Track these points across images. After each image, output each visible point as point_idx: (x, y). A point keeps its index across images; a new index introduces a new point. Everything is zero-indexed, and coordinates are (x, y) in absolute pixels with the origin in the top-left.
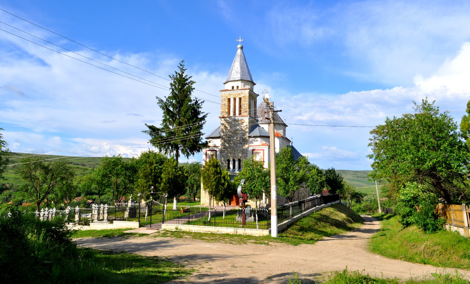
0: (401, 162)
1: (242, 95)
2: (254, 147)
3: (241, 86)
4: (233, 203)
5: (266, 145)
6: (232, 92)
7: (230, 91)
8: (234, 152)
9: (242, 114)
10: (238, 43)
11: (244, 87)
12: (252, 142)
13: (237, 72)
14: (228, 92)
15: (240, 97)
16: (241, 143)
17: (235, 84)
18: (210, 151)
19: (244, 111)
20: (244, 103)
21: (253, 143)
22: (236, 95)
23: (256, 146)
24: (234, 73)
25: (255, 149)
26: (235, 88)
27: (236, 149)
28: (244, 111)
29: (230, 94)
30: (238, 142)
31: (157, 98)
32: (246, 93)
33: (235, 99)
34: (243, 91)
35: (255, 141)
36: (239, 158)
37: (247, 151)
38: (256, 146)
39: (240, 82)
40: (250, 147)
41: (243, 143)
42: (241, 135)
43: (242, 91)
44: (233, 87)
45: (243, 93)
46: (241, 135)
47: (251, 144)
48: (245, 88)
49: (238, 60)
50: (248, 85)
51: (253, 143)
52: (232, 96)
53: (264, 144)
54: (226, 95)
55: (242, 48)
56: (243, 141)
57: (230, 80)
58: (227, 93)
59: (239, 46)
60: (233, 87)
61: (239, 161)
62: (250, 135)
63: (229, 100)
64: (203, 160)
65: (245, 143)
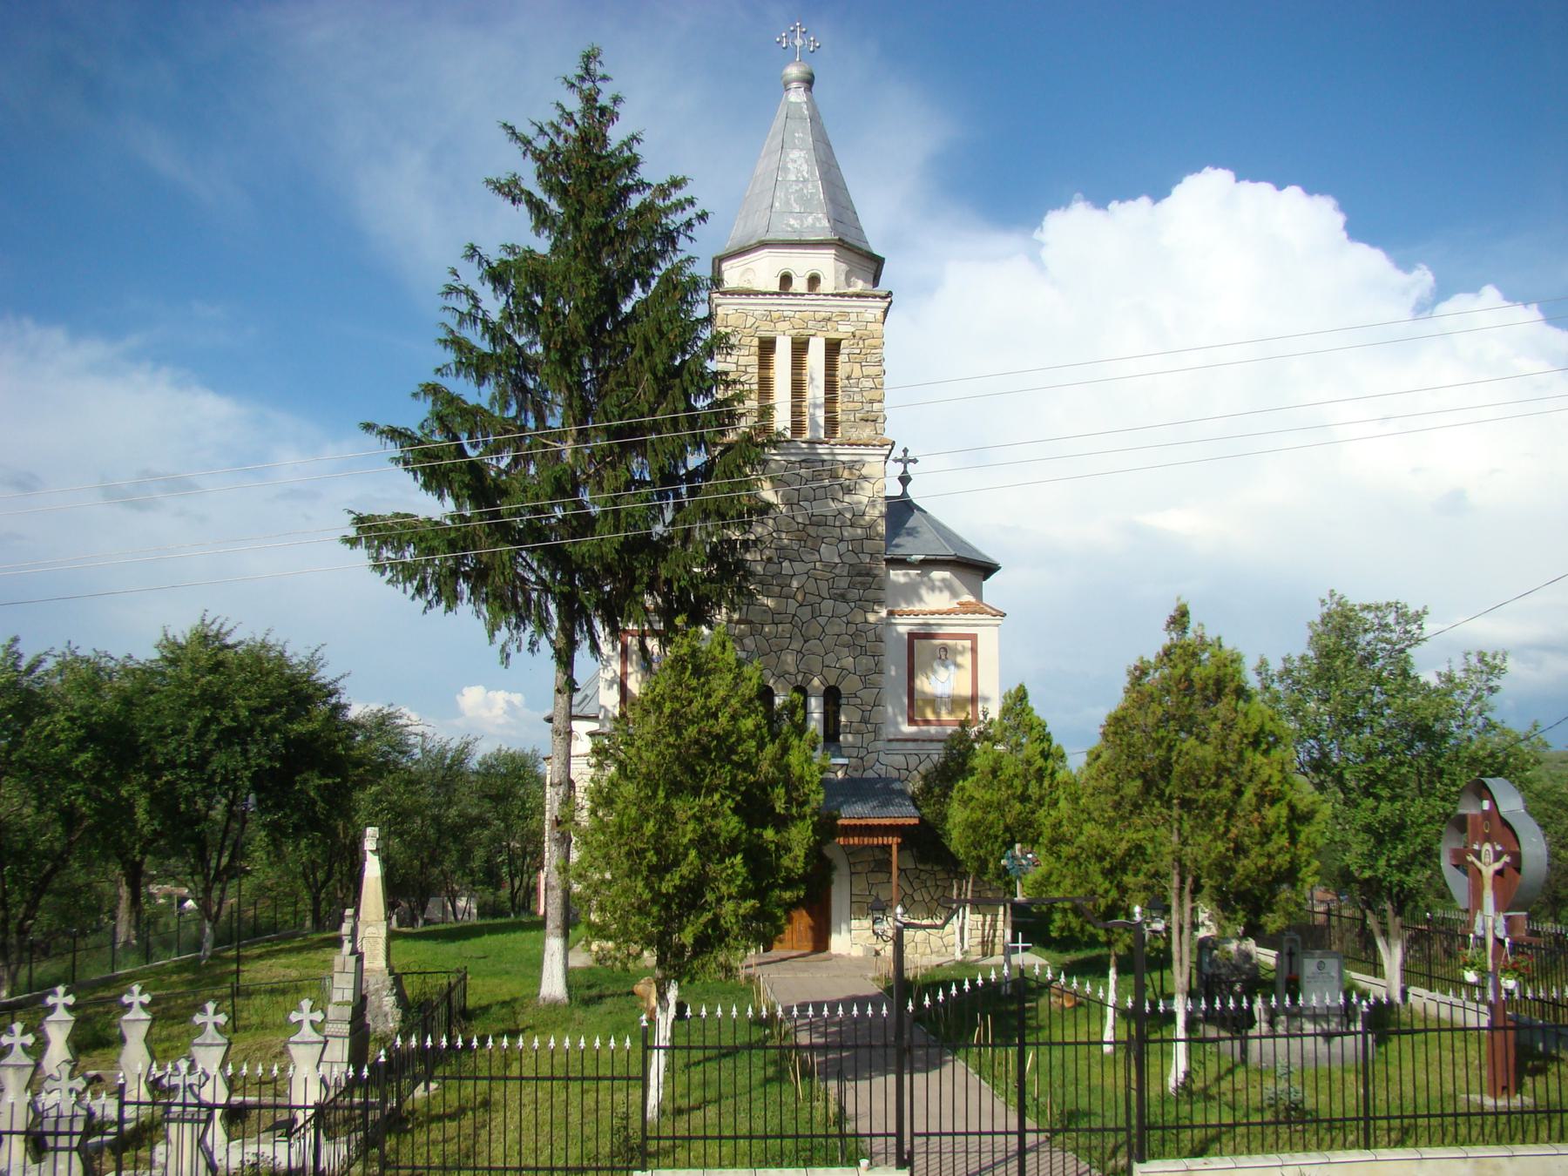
1: (841, 328)
3: (837, 278)
5: (988, 613)
6: (784, 305)
7: (768, 300)
8: (795, 646)
10: (789, 54)
11: (849, 286)
12: (911, 592)
13: (805, 201)
14: (760, 300)
15: (833, 335)
16: (843, 597)
17: (802, 264)
18: (497, 633)
20: (857, 372)
21: (920, 599)
22: (811, 324)
23: (933, 613)
24: (788, 202)
26: (799, 285)
27: (814, 629)
29: (775, 315)
30: (824, 585)
32: (870, 317)
33: (800, 348)
34: (855, 302)
35: (932, 588)
36: (832, 683)
37: (879, 639)
38: (933, 613)
39: (829, 254)
41: (854, 594)
42: (843, 547)
43: (846, 302)
44: (786, 280)
45: (853, 317)
47: (909, 602)
48: (851, 290)
49: (803, 140)
50: (865, 281)
51: (920, 599)
52: (781, 326)
53: (970, 603)
54: (750, 321)
55: (809, 82)
56: (851, 586)
57: (770, 237)
58: (757, 306)
59: (793, 71)
60: (786, 280)
61: (832, 697)
63: (767, 347)
65: (870, 594)
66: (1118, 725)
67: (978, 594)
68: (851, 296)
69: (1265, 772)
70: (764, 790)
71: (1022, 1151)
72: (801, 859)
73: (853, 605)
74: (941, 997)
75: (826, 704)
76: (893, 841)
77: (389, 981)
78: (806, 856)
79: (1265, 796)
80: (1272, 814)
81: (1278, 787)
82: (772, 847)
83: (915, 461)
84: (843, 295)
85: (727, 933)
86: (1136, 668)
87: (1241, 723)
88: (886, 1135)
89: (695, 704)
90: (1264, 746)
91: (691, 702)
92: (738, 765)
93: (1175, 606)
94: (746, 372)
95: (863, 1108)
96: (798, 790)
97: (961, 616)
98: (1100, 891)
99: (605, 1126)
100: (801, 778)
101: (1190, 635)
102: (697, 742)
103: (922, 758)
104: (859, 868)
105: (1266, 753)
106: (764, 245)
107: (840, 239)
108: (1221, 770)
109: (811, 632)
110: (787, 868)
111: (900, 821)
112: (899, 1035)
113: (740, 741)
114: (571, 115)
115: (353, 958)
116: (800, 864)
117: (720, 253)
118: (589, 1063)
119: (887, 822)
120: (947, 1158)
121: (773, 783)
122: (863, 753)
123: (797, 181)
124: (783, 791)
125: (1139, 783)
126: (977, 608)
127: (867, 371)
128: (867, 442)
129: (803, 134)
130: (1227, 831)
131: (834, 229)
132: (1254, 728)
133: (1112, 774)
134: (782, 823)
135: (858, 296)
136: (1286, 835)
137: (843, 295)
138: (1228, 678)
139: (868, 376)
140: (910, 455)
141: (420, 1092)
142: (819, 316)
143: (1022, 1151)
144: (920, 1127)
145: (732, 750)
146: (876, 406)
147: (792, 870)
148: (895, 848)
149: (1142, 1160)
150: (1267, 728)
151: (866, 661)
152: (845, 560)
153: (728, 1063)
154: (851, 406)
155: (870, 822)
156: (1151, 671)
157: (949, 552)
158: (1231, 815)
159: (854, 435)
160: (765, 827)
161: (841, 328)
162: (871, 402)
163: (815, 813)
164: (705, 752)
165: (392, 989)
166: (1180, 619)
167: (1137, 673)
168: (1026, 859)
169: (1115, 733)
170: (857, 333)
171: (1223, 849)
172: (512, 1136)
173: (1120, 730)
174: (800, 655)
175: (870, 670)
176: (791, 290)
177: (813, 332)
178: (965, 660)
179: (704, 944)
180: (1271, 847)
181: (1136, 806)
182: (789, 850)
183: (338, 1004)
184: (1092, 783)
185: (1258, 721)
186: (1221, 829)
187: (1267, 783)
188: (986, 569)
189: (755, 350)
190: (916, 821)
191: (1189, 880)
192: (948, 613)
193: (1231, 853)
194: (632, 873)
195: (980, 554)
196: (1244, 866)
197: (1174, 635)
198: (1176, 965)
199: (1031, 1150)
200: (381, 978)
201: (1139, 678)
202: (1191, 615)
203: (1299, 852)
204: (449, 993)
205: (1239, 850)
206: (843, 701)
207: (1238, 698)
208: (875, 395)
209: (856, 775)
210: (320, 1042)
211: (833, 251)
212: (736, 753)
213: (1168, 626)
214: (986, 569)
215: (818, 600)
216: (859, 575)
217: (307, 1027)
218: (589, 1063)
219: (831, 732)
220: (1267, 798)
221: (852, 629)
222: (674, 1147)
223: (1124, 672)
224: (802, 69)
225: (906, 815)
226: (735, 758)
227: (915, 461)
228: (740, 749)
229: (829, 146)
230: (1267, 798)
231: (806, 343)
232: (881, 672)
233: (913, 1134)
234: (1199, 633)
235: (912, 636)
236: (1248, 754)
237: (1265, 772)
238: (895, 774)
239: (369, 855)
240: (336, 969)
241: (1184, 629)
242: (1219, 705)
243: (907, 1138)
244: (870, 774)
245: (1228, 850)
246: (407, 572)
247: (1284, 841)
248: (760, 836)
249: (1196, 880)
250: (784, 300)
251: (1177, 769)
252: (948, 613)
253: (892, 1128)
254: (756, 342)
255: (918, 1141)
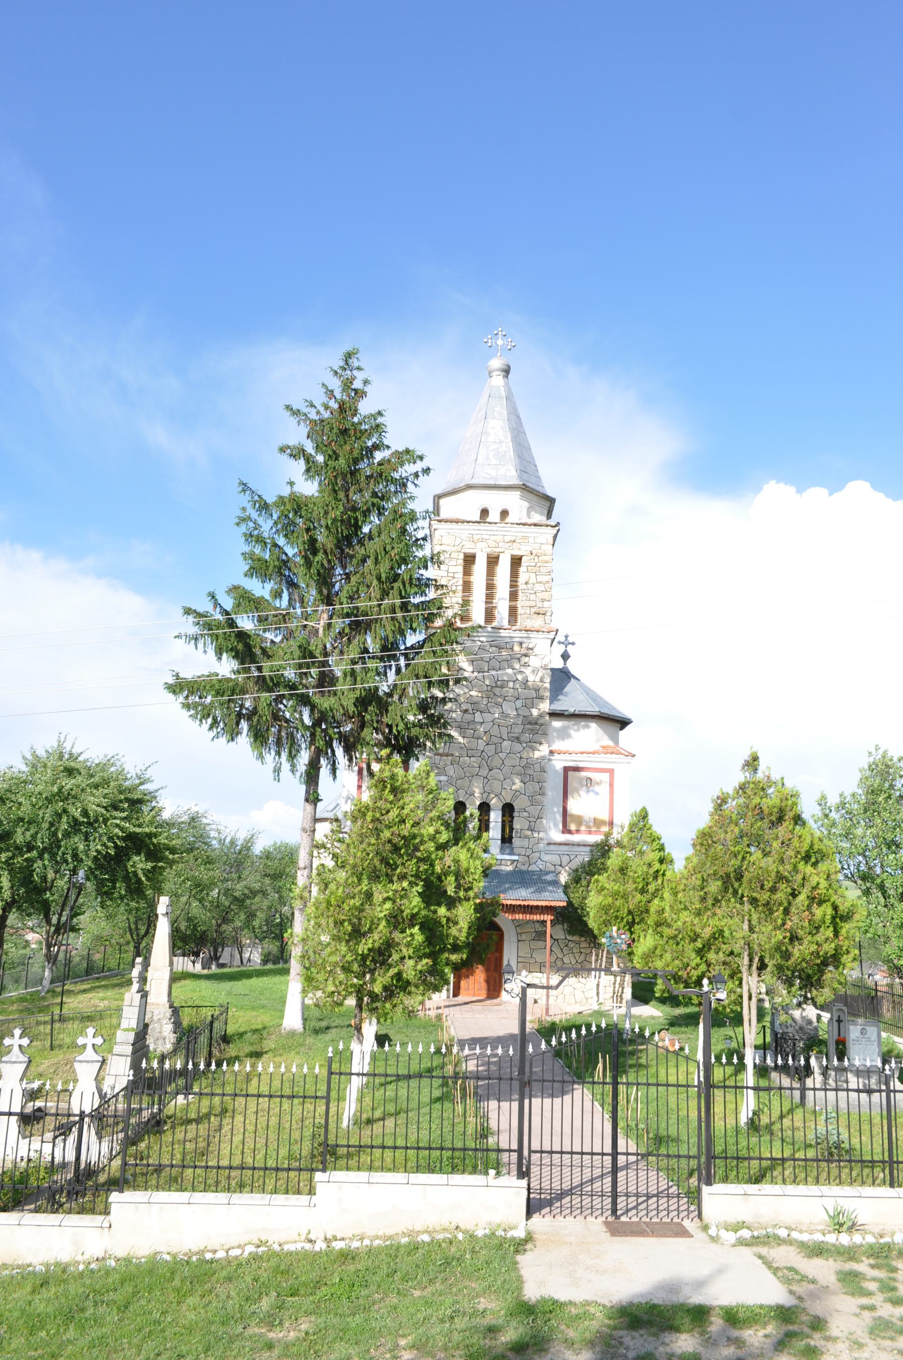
0: (884, 839)
1: (523, 548)
2: (574, 757)
4: (468, 989)
8: (484, 772)
9: (522, 621)
15: (517, 553)
17: (495, 501)
19: (533, 610)
20: (533, 580)
22: (501, 544)
23: (582, 753)
25: (581, 765)
26: (494, 516)
27: (496, 762)
28: (533, 610)
29: (476, 537)
30: (504, 731)
31: (244, 490)
33: (493, 561)
36: (508, 801)
38: (582, 753)
39: (517, 494)
40: (556, 756)
41: (526, 737)
42: (519, 703)
43: (526, 529)
44: (485, 512)
45: (531, 540)
46: (519, 703)
48: (530, 521)
50: (541, 514)
52: (480, 545)
53: (609, 747)
54: (458, 541)
55: (507, 371)
59: (496, 363)
60: (485, 512)
61: (508, 810)
62: (558, 707)
63: (469, 560)
64: (348, 798)
66: (705, 840)
67: (616, 740)
68: (530, 525)
69: (814, 880)
70: (439, 878)
71: (615, 1170)
72: (465, 930)
73: (524, 745)
74: (554, 1043)
75: (503, 816)
76: (548, 918)
77: (169, 1012)
78: (470, 928)
79: (815, 898)
80: (818, 912)
81: (824, 891)
82: (444, 921)
83: (573, 644)
84: (524, 524)
85: (408, 983)
86: (718, 798)
87: (795, 842)
88: (510, 1151)
89: (391, 813)
90: (813, 860)
91: (388, 812)
92: (420, 860)
93: (749, 753)
94: (454, 578)
95: (504, 1126)
96: (464, 879)
97: (603, 755)
98: (693, 964)
99: (308, 1133)
100: (467, 870)
101: (760, 775)
102: (390, 841)
103: (572, 857)
104: (524, 937)
105: (815, 865)
106: (469, 487)
107: (524, 484)
108: (780, 878)
109: (494, 764)
110: (455, 937)
111: (553, 904)
112: (522, 1071)
113: (422, 842)
114: (332, 391)
115: (139, 995)
116: (464, 934)
117: (439, 491)
118: (287, 1085)
119: (544, 904)
120: (556, 1170)
121: (446, 874)
122: (529, 852)
123: (495, 442)
124: (453, 878)
125: (719, 883)
126: (615, 750)
127: (540, 578)
128: (537, 628)
129: (501, 409)
130: (784, 924)
131: (520, 477)
132: (806, 847)
133: (699, 876)
134: (452, 903)
135: (535, 525)
136: (831, 929)
137: (524, 524)
138: (788, 808)
139: (540, 582)
140: (570, 640)
141: (181, 1099)
142: (507, 539)
143: (615, 1170)
144: (535, 1146)
145: (416, 849)
146: (546, 604)
147: (458, 939)
148: (549, 923)
149: (709, 1183)
150: (816, 847)
151: (532, 787)
152: (520, 712)
153: (414, 1083)
154: (528, 604)
155: (531, 903)
156: (730, 801)
157: (593, 709)
158: (786, 911)
159: (529, 624)
160: (439, 905)
161: (523, 548)
162: (543, 600)
163: (476, 897)
164: (396, 849)
165: (170, 1019)
166: (752, 763)
167: (719, 801)
168: (620, 939)
169: (702, 844)
170: (534, 552)
171: (781, 937)
172: (238, 1139)
173: (705, 842)
174: (486, 780)
175: (536, 792)
176: (488, 520)
177: (502, 550)
178: (604, 789)
179: (389, 992)
180: (820, 938)
181: (717, 901)
182: (456, 923)
183: (125, 1030)
184: (684, 881)
185: (808, 841)
186: (780, 922)
187: (814, 888)
188: (623, 723)
189: (461, 562)
190: (565, 904)
191: (756, 959)
192: (594, 753)
193: (787, 940)
194: (337, 938)
195: (618, 711)
196: (797, 951)
197: (747, 774)
198: (746, 1023)
199: (622, 1169)
200: (163, 1011)
201: (720, 805)
202: (761, 760)
203: (841, 943)
204: (212, 1023)
205: (794, 938)
206: (515, 814)
207: (796, 824)
208: (545, 595)
209: (524, 868)
210: (98, 1061)
211: (519, 493)
212: (419, 850)
213: (743, 768)
214: (623, 723)
215: (501, 741)
216: (530, 723)
217: (89, 1048)
218: (287, 1085)
219: (507, 836)
220: (816, 900)
221: (524, 762)
222: (359, 1152)
223: (710, 801)
224: (502, 362)
225: (558, 899)
226: (419, 854)
227: (573, 644)
228: (422, 848)
229: (518, 417)
230: (816, 900)
231: (498, 558)
232: (543, 794)
233: (530, 1151)
234: (767, 774)
235: (566, 770)
236: (801, 866)
237: (814, 880)
238: (552, 868)
239: (160, 917)
240: (126, 1003)
241: (755, 770)
242: (780, 828)
243: (526, 1153)
244: (533, 868)
245: (784, 938)
246: (205, 713)
247: (830, 933)
248: (435, 912)
249: (762, 959)
250: (483, 526)
251: (747, 876)
252: (594, 753)
253: (515, 1146)
254: (462, 556)
255: (535, 1157)
